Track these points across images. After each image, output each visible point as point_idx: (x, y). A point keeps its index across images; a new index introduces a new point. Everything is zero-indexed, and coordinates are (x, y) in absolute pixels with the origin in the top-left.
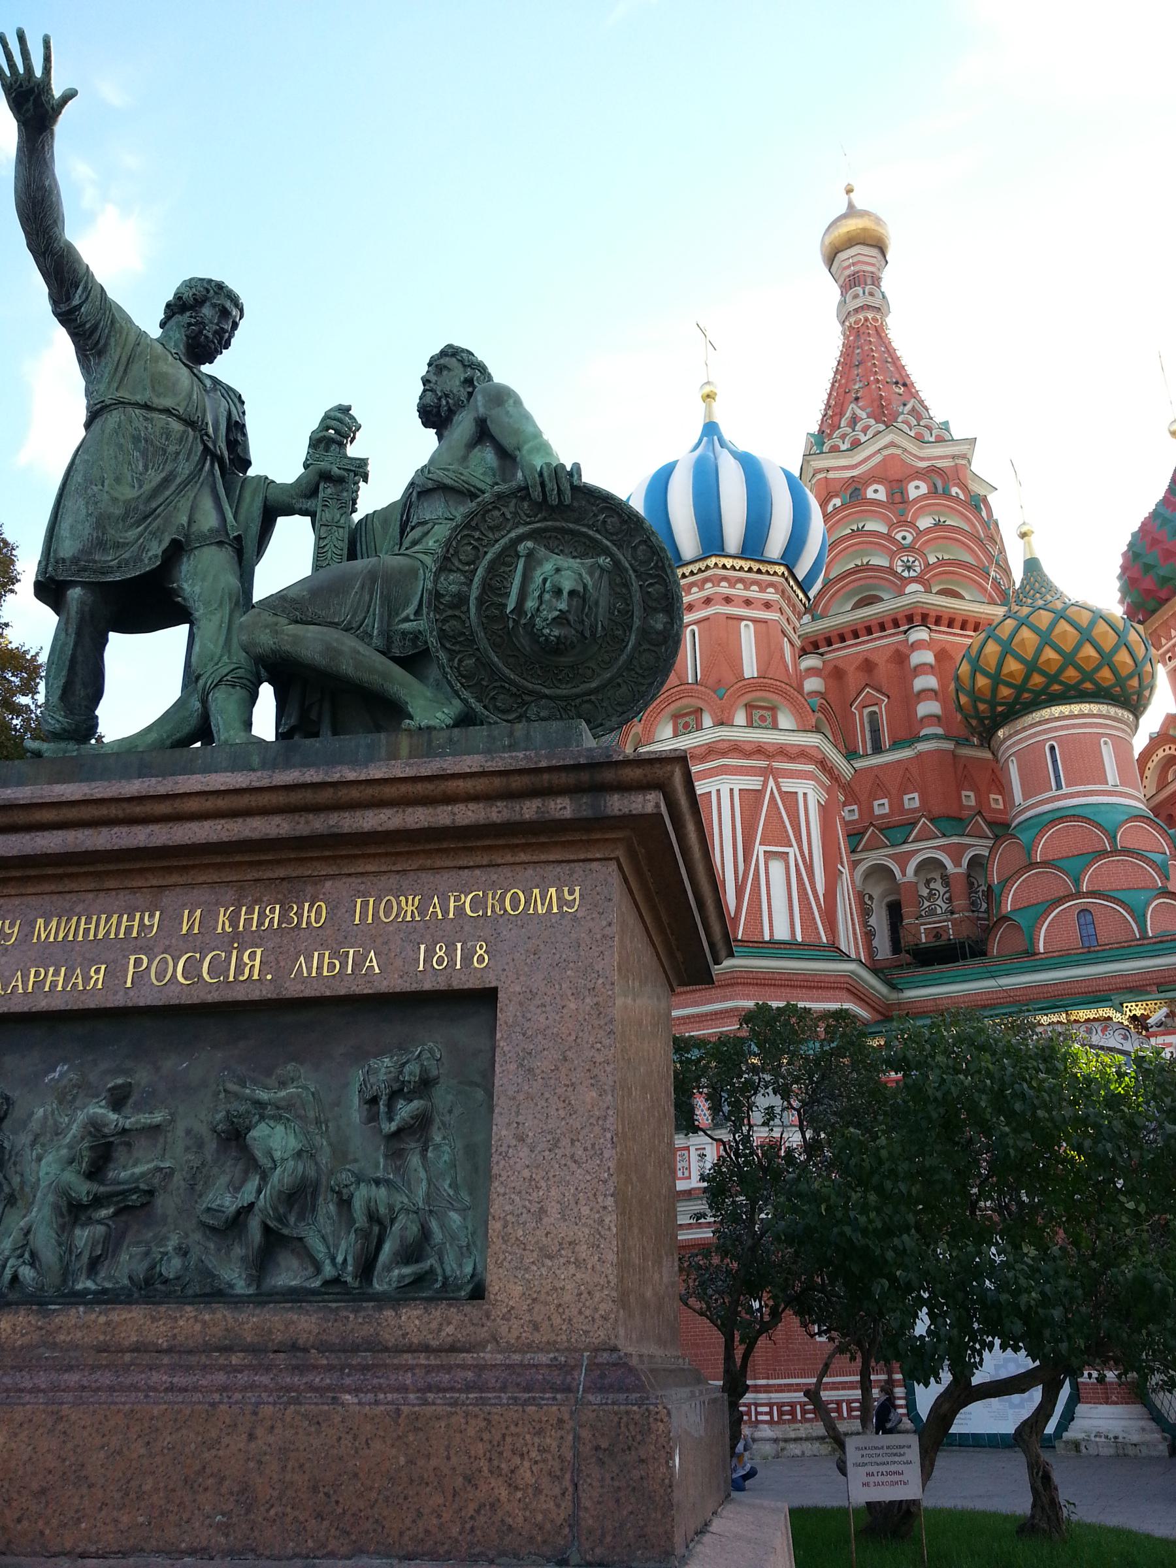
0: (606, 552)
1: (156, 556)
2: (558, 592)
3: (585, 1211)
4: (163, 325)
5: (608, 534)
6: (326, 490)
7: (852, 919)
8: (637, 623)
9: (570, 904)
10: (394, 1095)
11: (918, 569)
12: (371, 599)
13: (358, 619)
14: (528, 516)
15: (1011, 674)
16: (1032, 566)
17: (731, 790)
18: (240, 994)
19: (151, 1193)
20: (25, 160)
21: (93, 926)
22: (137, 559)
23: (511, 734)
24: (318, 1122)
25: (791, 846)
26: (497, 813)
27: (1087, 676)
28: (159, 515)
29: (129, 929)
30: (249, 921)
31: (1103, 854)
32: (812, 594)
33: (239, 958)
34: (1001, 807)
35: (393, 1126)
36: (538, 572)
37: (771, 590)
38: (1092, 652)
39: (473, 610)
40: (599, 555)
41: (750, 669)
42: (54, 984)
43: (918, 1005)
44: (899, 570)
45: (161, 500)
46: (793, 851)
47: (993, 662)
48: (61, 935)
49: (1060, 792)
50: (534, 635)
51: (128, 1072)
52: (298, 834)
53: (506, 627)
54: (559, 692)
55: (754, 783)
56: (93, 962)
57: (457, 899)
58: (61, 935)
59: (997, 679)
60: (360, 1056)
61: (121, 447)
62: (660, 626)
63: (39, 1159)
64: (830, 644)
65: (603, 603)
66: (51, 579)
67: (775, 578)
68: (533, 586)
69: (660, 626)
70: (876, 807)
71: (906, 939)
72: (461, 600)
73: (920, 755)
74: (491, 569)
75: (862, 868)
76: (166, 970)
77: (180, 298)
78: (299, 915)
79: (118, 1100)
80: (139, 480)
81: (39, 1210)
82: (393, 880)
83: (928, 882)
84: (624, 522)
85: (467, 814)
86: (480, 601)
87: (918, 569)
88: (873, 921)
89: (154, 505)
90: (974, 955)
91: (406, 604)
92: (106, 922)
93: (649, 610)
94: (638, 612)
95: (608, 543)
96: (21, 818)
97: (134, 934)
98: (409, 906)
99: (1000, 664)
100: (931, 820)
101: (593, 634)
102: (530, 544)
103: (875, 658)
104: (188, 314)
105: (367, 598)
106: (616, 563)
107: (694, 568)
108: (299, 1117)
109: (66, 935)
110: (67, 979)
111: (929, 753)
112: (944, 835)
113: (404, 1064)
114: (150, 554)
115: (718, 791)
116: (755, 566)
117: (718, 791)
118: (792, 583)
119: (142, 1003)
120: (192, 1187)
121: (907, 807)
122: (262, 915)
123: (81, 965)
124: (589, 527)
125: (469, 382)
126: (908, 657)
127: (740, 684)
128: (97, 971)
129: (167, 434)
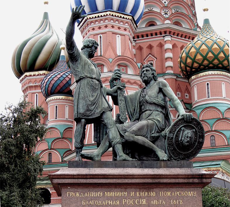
2: (188, 137)
4: (82, 49)
5: (194, 125)
6: (119, 92)
8: (198, 141)
9: (194, 194)
11: (169, 14)
12: (148, 130)
13: (146, 134)
14: (183, 123)
15: (198, 60)
16: (206, 21)
20: (72, 25)
21: (115, 194)
22: (94, 113)
23: (181, 163)
26: (186, 181)
27: (221, 63)
28: (97, 104)
29: (122, 195)
30: (142, 194)
31: (220, 119)
32: (137, 25)
33: (142, 201)
36: (184, 133)
37: (127, 24)
39: (174, 140)
40: (193, 129)
41: (119, 53)
42: (110, 203)
44: (163, 14)
47: (193, 55)
48: (110, 195)
52: (153, 182)
53: (179, 143)
54: (185, 153)
56: (116, 200)
58: (110, 195)
59: (194, 61)
61: (89, 88)
62: (201, 141)
67: (128, 20)
68: (183, 135)
69: (201, 141)
72: (172, 138)
77: (89, 45)
78: (151, 194)
82: (166, 189)
86: (175, 138)
91: (152, 131)
92: (118, 193)
93: (200, 138)
95: (195, 127)
96: (106, 177)
97: (123, 196)
98: (169, 194)
101: (191, 143)
102: (183, 128)
103: (153, 44)
104: (90, 49)
106: (196, 130)
107: (102, 14)
109: (111, 195)
110: (113, 203)
112: (172, 107)
114: (96, 112)
116: (123, 16)
118: (133, 22)
122: (144, 193)
123: (114, 200)
124: (192, 124)
125: (153, 74)
126: (164, 45)
128: (118, 202)
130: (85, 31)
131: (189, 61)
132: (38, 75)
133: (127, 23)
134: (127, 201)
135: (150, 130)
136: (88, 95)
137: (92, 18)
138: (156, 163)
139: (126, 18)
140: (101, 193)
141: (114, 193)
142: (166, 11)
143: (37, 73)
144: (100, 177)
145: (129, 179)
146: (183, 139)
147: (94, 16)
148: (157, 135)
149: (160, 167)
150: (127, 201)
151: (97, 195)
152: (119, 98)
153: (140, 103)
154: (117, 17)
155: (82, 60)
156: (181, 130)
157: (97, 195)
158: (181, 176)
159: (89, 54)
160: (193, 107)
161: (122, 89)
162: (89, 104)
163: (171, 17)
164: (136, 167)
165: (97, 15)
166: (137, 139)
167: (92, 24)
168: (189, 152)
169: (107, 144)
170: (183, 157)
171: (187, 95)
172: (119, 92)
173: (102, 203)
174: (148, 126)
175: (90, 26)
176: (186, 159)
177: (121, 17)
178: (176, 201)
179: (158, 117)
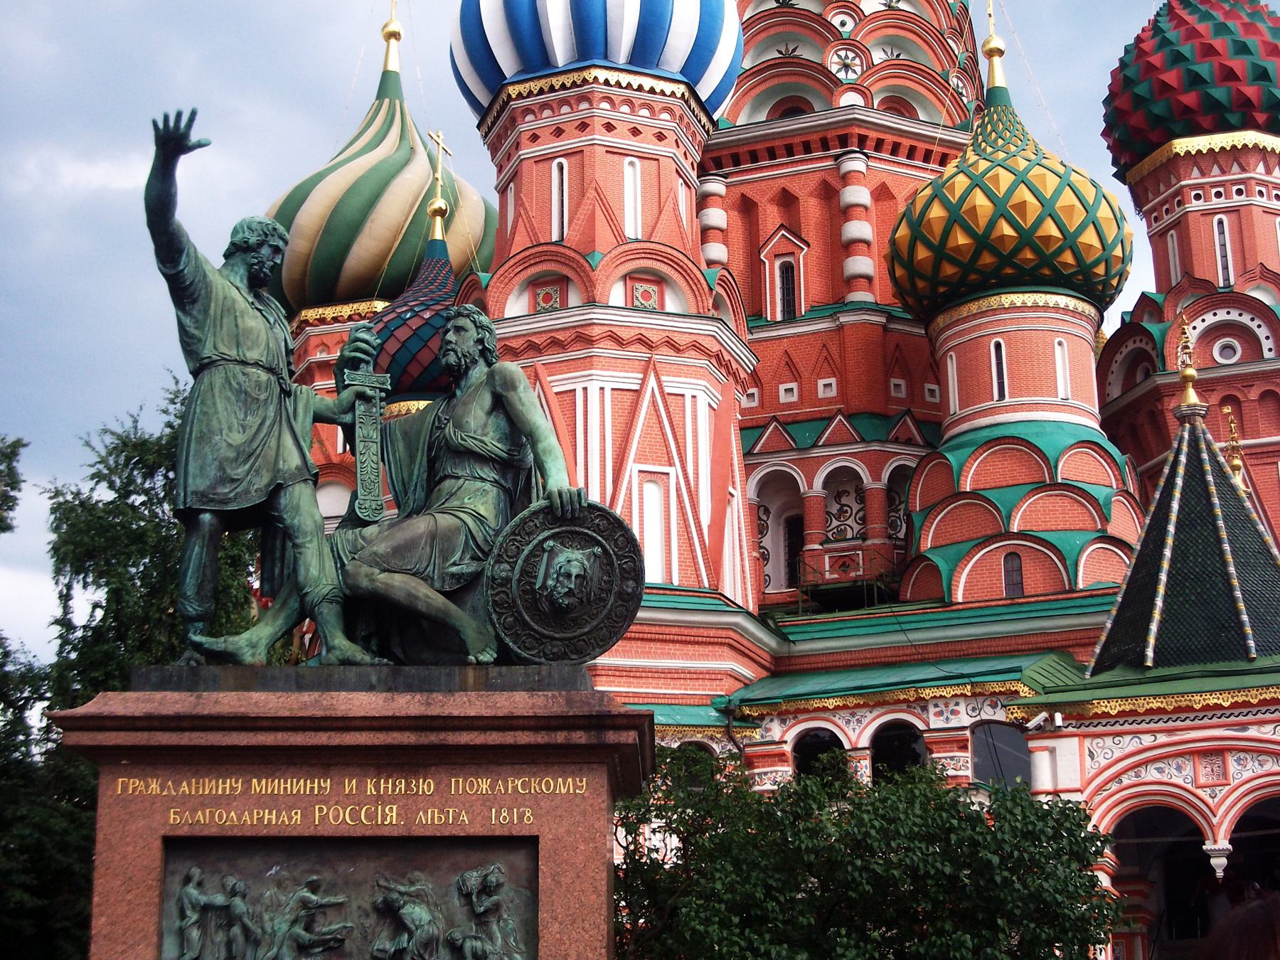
0: (599, 544)
1: (260, 489)
2: (569, 576)
3: (590, 955)
4: (228, 255)
5: (600, 532)
6: (360, 408)
7: (741, 554)
10: (480, 893)
13: (424, 565)
17: (602, 389)
18: (386, 832)
19: (342, 941)
22: (247, 492)
23: (539, 673)
24: (436, 905)
25: (671, 464)
26: (540, 738)
29: (312, 789)
31: (1040, 487)
32: (716, 117)
33: (383, 811)
34: (937, 400)
35: (482, 909)
36: (556, 561)
37: (666, 116)
38: (1055, 232)
39: (514, 586)
41: (633, 227)
43: (813, 660)
45: (258, 441)
46: (674, 472)
47: (938, 229)
49: (1002, 403)
50: (552, 601)
51: (317, 872)
55: (630, 380)
56: (291, 808)
57: (513, 782)
59: (941, 251)
60: (456, 868)
61: (228, 399)
62: (630, 590)
63: (272, 920)
64: (737, 163)
65: (595, 579)
66: (190, 508)
70: (782, 392)
71: (810, 578)
73: (841, 328)
74: (525, 561)
75: (758, 474)
76: (338, 816)
79: (314, 887)
80: (243, 426)
81: (280, 948)
83: (838, 497)
84: (610, 523)
85: (524, 738)
86: (519, 581)
87: (858, 69)
88: (767, 542)
89: (255, 445)
90: (882, 600)
91: (453, 553)
93: (624, 579)
94: (617, 581)
98: (484, 785)
99: (946, 233)
100: (849, 417)
102: (551, 543)
103: (795, 188)
105: (428, 549)
107: (567, 79)
108: (423, 901)
110: (278, 817)
111: (854, 325)
112: (863, 440)
113: (486, 876)
115: (585, 389)
116: (647, 83)
117: (585, 389)
118: (693, 104)
119: (326, 834)
120: (365, 938)
121: (821, 394)
122: (394, 785)
125: (481, 341)
127: (620, 250)
129: (258, 385)
130: (507, 144)
131: (922, 253)
132: (350, 318)
133: (668, 110)
134: (329, 809)
135: (441, 551)
136: (225, 426)
137: (528, 96)
138: (448, 675)
139: (663, 93)
140: (237, 782)
141: (286, 783)
142: (847, 57)
143: (346, 310)
144: (226, 723)
145: (333, 734)
146: (550, 582)
147: (534, 86)
148: (471, 569)
149: (464, 688)
150: (329, 809)
151: (224, 789)
152: (359, 432)
153: (430, 450)
154: (626, 88)
155: (213, 296)
156: (544, 550)
157: (224, 789)
158: (521, 722)
159: (250, 272)
160: (946, 437)
161: (374, 398)
162: (227, 459)
163: (865, 79)
164: (371, 688)
165: (542, 83)
166: (387, 584)
167: (530, 117)
168: (579, 632)
169: (294, 604)
170: (555, 650)
171: (932, 392)
172: (360, 408)
173: (239, 819)
174: (433, 536)
175: (523, 127)
176: (574, 657)
177: (640, 88)
178: (510, 811)
179: (478, 498)
